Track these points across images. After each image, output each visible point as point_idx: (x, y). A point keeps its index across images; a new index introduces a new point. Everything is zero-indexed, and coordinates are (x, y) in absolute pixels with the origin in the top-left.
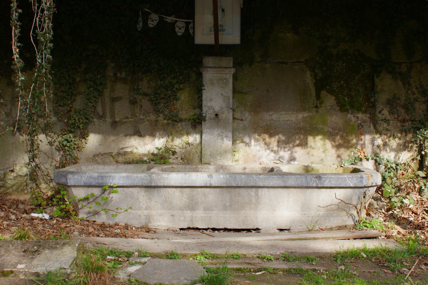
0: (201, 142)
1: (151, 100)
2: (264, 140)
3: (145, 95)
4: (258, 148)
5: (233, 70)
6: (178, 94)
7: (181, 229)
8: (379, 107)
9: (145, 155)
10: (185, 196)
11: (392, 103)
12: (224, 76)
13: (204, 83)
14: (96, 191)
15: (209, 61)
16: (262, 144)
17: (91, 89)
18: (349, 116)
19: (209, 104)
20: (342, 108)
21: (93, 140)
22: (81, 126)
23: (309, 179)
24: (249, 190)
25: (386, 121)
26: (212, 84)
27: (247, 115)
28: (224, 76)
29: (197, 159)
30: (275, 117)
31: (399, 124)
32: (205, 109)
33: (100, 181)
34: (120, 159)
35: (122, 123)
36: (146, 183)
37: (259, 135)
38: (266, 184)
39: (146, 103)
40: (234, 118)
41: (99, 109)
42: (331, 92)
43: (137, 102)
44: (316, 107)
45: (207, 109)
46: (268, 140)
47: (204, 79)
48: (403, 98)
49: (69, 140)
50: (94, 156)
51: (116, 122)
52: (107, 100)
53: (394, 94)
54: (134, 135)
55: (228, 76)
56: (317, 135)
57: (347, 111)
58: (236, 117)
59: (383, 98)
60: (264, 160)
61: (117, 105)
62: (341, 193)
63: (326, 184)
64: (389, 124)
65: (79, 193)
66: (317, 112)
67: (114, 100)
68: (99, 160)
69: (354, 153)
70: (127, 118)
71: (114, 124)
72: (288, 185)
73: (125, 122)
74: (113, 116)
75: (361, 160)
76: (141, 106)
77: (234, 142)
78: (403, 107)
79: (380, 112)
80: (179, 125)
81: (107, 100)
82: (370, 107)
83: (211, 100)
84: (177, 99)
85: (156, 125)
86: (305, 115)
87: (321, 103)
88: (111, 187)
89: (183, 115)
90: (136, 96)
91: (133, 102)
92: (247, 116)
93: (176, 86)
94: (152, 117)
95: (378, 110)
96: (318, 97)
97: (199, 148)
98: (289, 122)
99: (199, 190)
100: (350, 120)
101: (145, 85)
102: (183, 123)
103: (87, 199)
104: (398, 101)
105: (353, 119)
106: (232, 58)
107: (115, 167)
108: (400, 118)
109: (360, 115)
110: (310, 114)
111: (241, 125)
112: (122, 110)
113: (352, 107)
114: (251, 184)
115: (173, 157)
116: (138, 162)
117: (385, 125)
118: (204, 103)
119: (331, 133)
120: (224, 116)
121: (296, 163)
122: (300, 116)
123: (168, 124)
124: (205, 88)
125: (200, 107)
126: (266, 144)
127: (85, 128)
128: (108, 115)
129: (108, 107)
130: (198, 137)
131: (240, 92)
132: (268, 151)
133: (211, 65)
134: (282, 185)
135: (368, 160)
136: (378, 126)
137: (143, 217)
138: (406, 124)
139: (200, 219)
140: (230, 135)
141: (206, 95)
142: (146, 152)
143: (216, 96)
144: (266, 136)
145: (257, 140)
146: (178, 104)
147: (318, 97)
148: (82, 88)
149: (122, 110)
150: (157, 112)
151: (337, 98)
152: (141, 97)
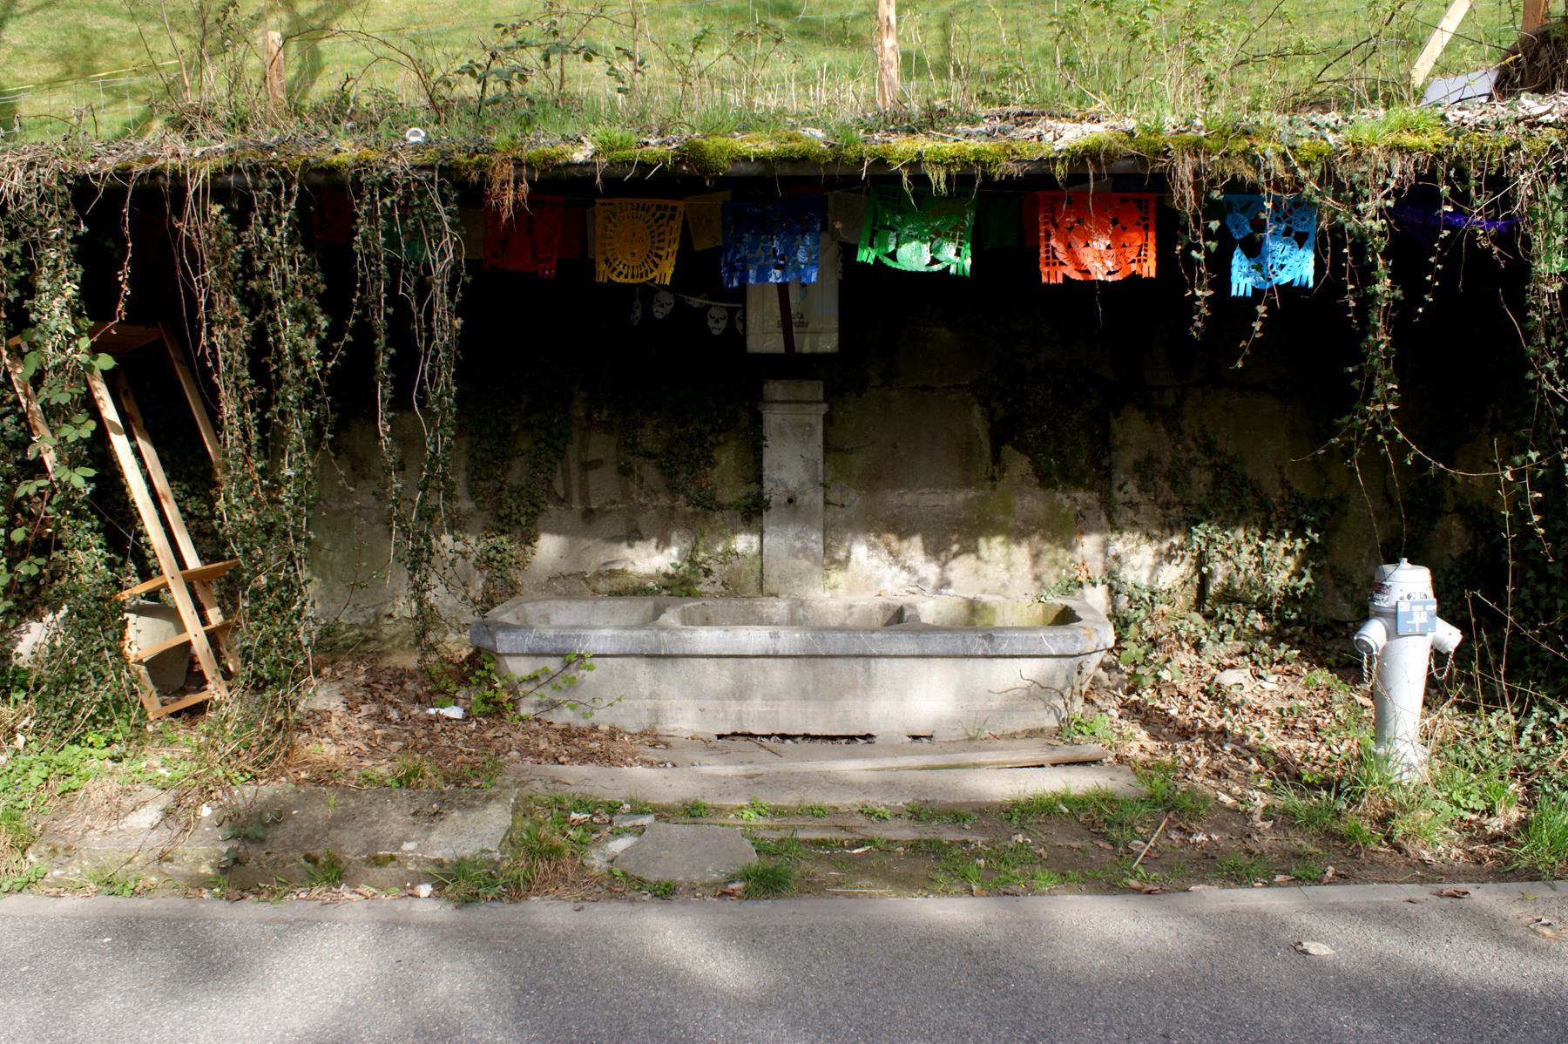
0: (761, 552)
1: (660, 467)
2: (888, 545)
3: (649, 455)
4: (875, 561)
5: (824, 408)
6: (715, 454)
7: (720, 737)
8: (1119, 476)
9: (650, 577)
10: (726, 673)
11: (1144, 470)
12: (807, 419)
13: (766, 433)
14: (553, 664)
15: (775, 389)
16: (884, 555)
17: (542, 445)
18: (1059, 496)
20: (1045, 480)
21: (549, 547)
22: (523, 520)
23: (969, 640)
24: (852, 661)
25: (1131, 505)
26: (783, 434)
27: (853, 494)
28: (807, 419)
29: (752, 587)
30: (909, 499)
31: (1158, 511)
32: (767, 486)
33: (560, 646)
34: (602, 585)
35: (603, 512)
36: (648, 649)
37: (878, 537)
38: (884, 651)
39: (651, 474)
40: (827, 503)
41: (558, 485)
42: (1022, 447)
43: (632, 471)
44: (993, 478)
45: (772, 485)
46: (895, 545)
47: (766, 424)
48: (1167, 459)
49: (500, 548)
50: (550, 579)
51: (591, 511)
52: (574, 466)
53: (1150, 452)
55: (813, 420)
56: (994, 535)
57: (1054, 486)
58: (832, 498)
59: (1127, 458)
60: (887, 586)
61: (593, 475)
62: (1031, 669)
63: (1004, 649)
64: (1137, 512)
65: (519, 668)
66: (994, 488)
67: (586, 466)
68: (560, 589)
69: (1069, 572)
70: (614, 502)
71: (589, 515)
72: (927, 652)
73: (610, 511)
74: (585, 498)
75: (1081, 585)
76: (642, 479)
78: (1166, 477)
79: (1120, 488)
80: (718, 515)
81: (574, 466)
82: (1100, 477)
83: (780, 467)
84: (713, 465)
85: (671, 517)
86: (970, 495)
87: (1002, 471)
88: (581, 656)
89: (726, 496)
90: (630, 458)
91: (625, 471)
92: (854, 498)
93: (710, 438)
94: (664, 501)
95: (1117, 484)
96: (996, 458)
97: (758, 562)
98: (937, 510)
99: (753, 661)
100: (1061, 505)
101: (648, 437)
102: (726, 513)
103: (534, 679)
104: (1157, 466)
105: (1067, 503)
106: (821, 383)
107: (590, 603)
108: (1160, 501)
109: (1080, 495)
110: (980, 493)
112: (603, 486)
113: (1065, 478)
114: (856, 651)
116: (637, 590)
117: (1131, 514)
118: (766, 473)
119: (1021, 531)
120: (806, 499)
121: (951, 591)
122: (960, 497)
123: (695, 514)
124: (769, 443)
125: (759, 480)
126: (891, 553)
127: (531, 524)
128: (576, 496)
129: (575, 482)
130: (755, 539)
131: (838, 450)
132: (896, 569)
133: (779, 396)
134: (917, 652)
135: (1094, 585)
136: (1115, 517)
137: (645, 714)
138: (1173, 511)
139: (757, 715)
141: (769, 457)
142: (652, 571)
143: (790, 461)
144: (892, 538)
145: (872, 546)
146: (715, 474)
147: (996, 458)
148: (524, 445)
149: (603, 486)
150: (673, 489)
151: (1034, 462)
152: (640, 460)
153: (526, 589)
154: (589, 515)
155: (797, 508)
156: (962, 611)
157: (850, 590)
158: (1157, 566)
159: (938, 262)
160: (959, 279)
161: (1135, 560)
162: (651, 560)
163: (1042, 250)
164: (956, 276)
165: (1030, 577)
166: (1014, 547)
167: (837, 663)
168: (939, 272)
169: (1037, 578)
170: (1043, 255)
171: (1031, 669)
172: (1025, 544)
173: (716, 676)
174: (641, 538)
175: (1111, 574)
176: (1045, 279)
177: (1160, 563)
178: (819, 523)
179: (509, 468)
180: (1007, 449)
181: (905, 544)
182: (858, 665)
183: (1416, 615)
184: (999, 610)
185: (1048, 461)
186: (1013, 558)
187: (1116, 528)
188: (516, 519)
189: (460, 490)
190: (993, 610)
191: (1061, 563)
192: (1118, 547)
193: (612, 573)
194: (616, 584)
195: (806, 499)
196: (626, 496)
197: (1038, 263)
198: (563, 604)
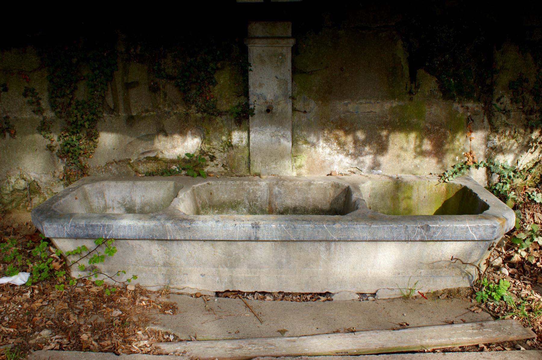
0: (248, 145)
1: (177, 86)
2: (337, 138)
3: (170, 78)
4: (328, 150)
5: (292, 42)
6: (216, 76)
7: (218, 294)
8: (498, 91)
9: (173, 162)
10: (219, 250)
11: (516, 88)
12: (280, 50)
13: (251, 61)
14: (90, 244)
15: (257, 29)
16: (335, 145)
17: (97, 72)
18: (456, 105)
19: (258, 91)
20: (447, 94)
22: (86, 124)
23: (410, 230)
24: (317, 244)
25: (506, 112)
26: (262, 62)
28: (280, 50)
29: (243, 169)
30: (351, 107)
31: (523, 116)
32: (252, 99)
33: (91, 233)
34: (142, 168)
35: (140, 118)
40: (294, 110)
41: (109, 100)
42: (431, 71)
43: (159, 89)
44: (410, 93)
45: (255, 98)
47: (250, 54)
48: (532, 79)
49: (72, 143)
50: (107, 164)
51: (132, 117)
52: (119, 87)
53: (521, 74)
54: (158, 133)
55: (284, 51)
57: (453, 98)
58: (298, 107)
59: (504, 79)
60: (336, 168)
61: (133, 92)
63: (437, 236)
64: (508, 117)
65: (65, 246)
66: (411, 99)
67: (128, 86)
68: (114, 170)
69: (461, 158)
70: (147, 111)
71: (131, 120)
73: (145, 118)
74: (128, 109)
75: (468, 168)
76: (166, 95)
78: (531, 92)
79: (498, 100)
80: (218, 119)
81: (119, 87)
82: (485, 93)
83: (261, 85)
84: (215, 84)
85: (187, 121)
86: (394, 105)
87: (417, 87)
89: (223, 106)
90: (157, 80)
91: (154, 89)
92: (313, 106)
93: (212, 65)
94: (181, 109)
95: (496, 97)
96: (413, 78)
97: (246, 152)
98: (371, 115)
99: (239, 243)
100: (457, 112)
101: (169, 65)
102: (224, 118)
103: (76, 253)
104: (525, 84)
105: (461, 110)
106: (290, 23)
107: (130, 183)
108: (526, 108)
109: (470, 105)
110: (402, 103)
111: (304, 120)
112: (139, 99)
113: (460, 92)
115: (212, 164)
116: (164, 170)
117: (504, 118)
118: (251, 89)
119: (429, 130)
120: (280, 108)
121: (380, 171)
122: (387, 106)
123: (203, 119)
124: (252, 68)
125: (246, 94)
127: (92, 127)
128: (121, 107)
130: (245, 135)
131: (302, 72)
132: (341, 156)
133: (259, 34)
134: (369, 238)
135: (477, 167)
136: (493, 120)
138: (533, 116)
139: (244, 279)
140: (289, 134)
141: (253, 78)
142: (175, 157)
143: (267, 82)
145: (327, 140)
146: (216, 90)
147: (413, 78)
149: (139, 99)
150: (187, 101)
151: (440, 81)
152: (164, 81)
157: (310, 171)
178: (289, 125)
179: (76, 88)
180: (421, 72)
182: (322, 247)
184: (415, 187)
188: (82, 123)
189: (44, 104)
190: (411, 188)
194: (151, 166)
195: (280, 108)
198: (113, 183)
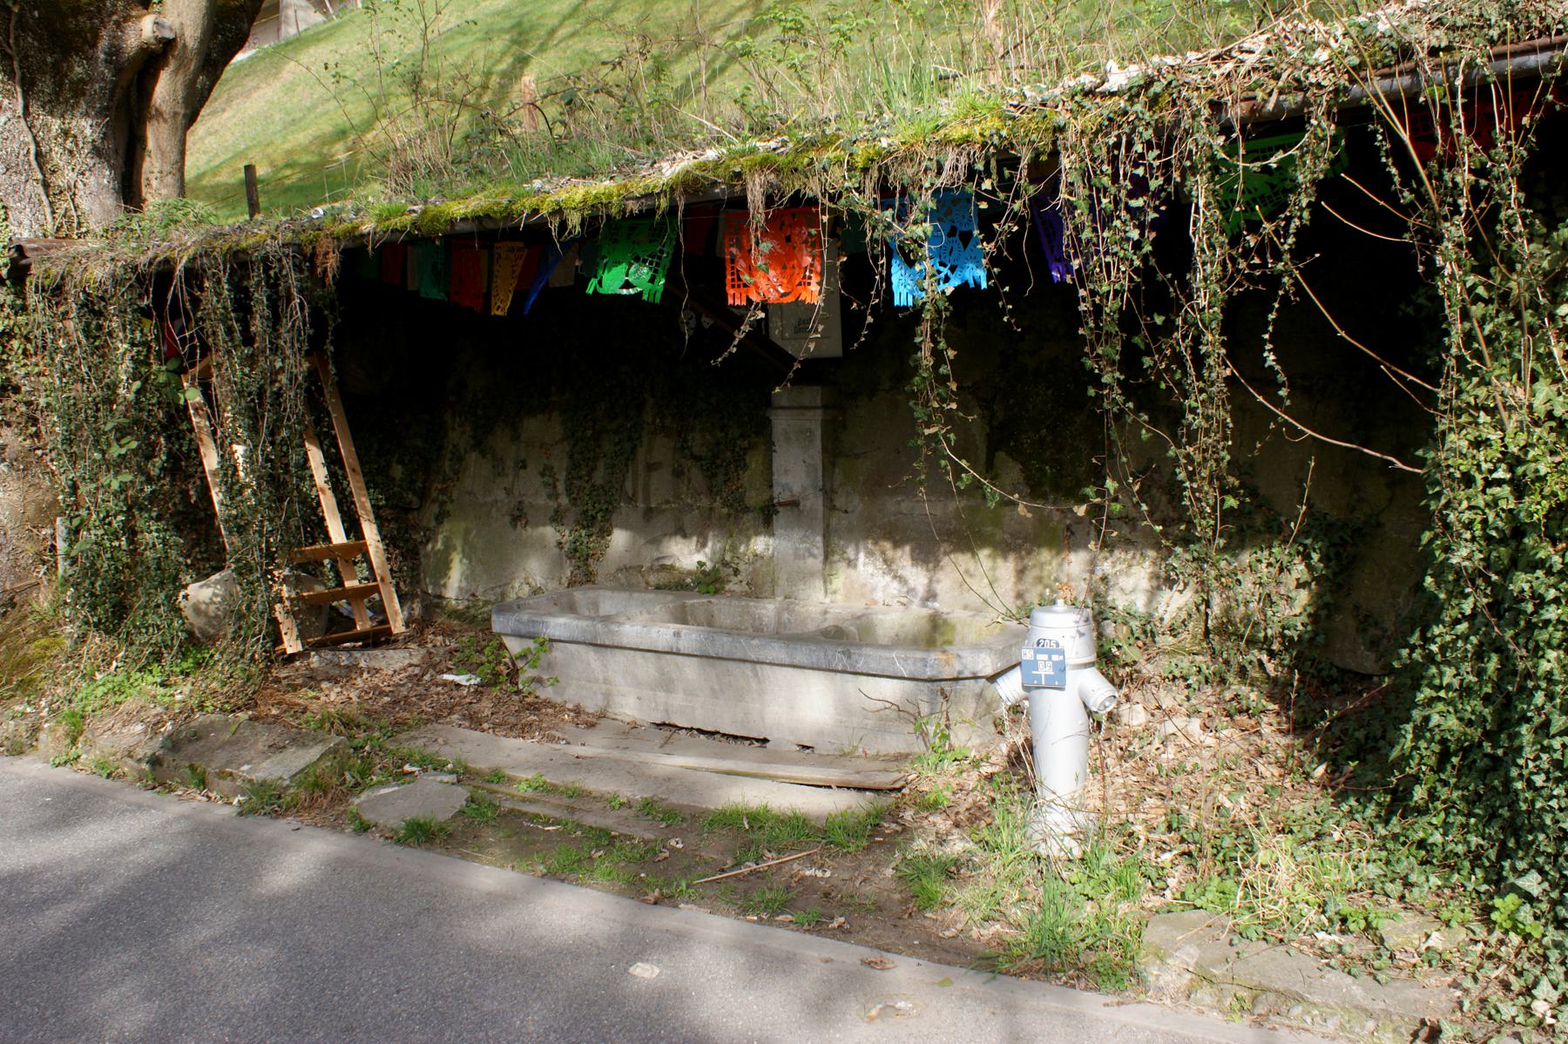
2: (883, 553)
4: (870, 569)
16: (880, 563)
19: (784, 481)
27: (856, 500)
34: (653, 579)
36: (589, 638)
37: (876, 543)
38: (762, 658)
39: (696, 475)
41: (628, 485)
42: (1016, 454)
46: (890, 553)
50: (619, 570)
54: (676, 534)
56: (981, 547)
61: (655, 475)
62: (890, 690)
63: (860, 667)
67: (651, 467)
70: (668, 502)
71: (649, 513)
72: (796, 662)
74: (647, 499)
77: (827, 556)
81: (641, 467)
83: (786, 472)
85: (710, 518)
88: (551, 640)
91: (678, 473)
92: (857, 504)
94: (705, 502)
105: (1057, 516)
110: (972, 503)
111: (844, 522)
112: (661, 483)
113: (1056, 488)
114: (739, 655)
115: (735, 579)
120: (808, 504)
123: (729, 515)
126: (885, 561)
128: (640, 495)
129: (641, 482)
132: (888, 578)
134: (787, 661)
137: (600, 696)
140: (819, 539)
143: (794, 466)
144: (887, 545)
145: (870, 554)
146: (745, 477)
148: (608, 447)
149: (661, 483)
150: (712, 492)
151: (1025, 469)
153: (599, 579)
154: (649, 513)
155: (801, 512)
156: (924, 625)
157: (847, 597)
158: (1154, 592)
159: (632, 286)
160: (650, 306)
161: (1126, 582)
162: (687, 555)
163: (729, 272)
164: (647, 303)
165: (1012, 594)
166: (1000, 561)
167: (731, 665)
168: (630, 296)
169: (1019, 596)
170: (729, 277)
171: (890, 690)
172: (1012, 557)
173: (646, 667)
174: (685, 536)
175: (1098, 597)
176: (730, 301)
177: (1159, 588)
178: (820, 527)
179: (594, 468)
180: (1001, 455)
181: (899, 553)
182: (748, 668)
183: (1041, 665)
184: (958, 627)
185: (1042, 470)
186: (998, 573)
187: (1108, 546)
189: (561, 487)
190: (953, 627)
191: (1046, 581)
192: (1106, 567)
193: (664, 567)
194: (663, 577)
195: (808, 504)
196: (678, 497)
197: (725, 285)
198: (608, 593)
